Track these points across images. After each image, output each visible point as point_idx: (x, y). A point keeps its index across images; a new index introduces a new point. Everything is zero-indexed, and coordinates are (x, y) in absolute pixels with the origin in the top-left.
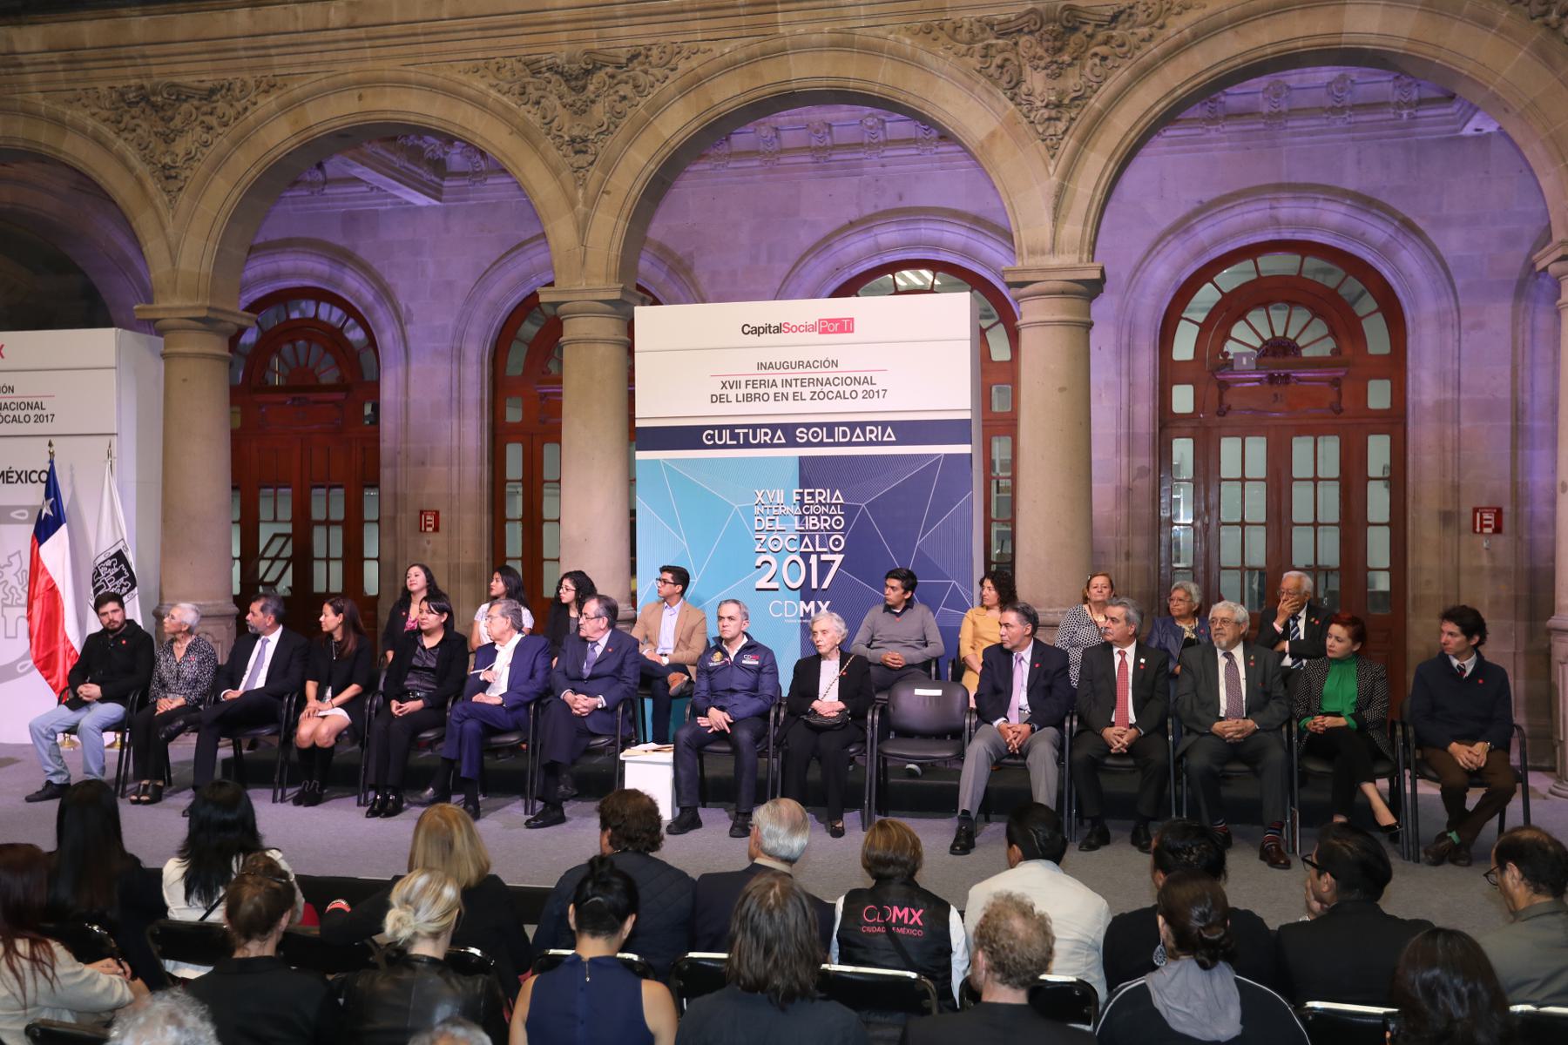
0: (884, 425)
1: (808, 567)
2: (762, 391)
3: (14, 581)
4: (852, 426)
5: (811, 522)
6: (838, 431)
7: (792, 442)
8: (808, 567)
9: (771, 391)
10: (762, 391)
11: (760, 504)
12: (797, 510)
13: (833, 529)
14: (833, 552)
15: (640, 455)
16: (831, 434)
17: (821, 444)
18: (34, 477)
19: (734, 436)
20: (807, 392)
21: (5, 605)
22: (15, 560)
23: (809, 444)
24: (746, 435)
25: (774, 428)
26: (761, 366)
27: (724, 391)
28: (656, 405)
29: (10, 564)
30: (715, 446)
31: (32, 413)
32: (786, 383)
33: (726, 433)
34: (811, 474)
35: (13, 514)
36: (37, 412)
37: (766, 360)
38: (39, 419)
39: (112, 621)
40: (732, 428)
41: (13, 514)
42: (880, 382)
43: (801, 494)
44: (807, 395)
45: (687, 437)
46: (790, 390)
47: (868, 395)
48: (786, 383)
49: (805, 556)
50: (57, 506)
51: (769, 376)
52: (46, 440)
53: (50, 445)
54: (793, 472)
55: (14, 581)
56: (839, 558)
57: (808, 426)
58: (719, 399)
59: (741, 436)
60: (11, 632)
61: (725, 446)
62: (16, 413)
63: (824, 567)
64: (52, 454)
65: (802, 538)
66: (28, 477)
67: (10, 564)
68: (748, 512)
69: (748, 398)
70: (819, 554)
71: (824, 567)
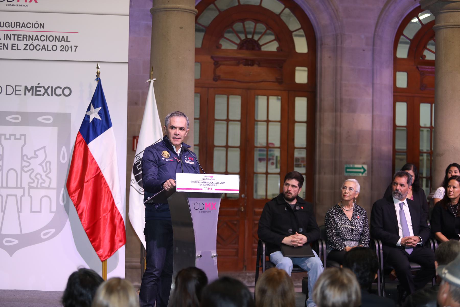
3: (39, 169)
18: (59, 91)
21: (30, 188)
22: (41, 154)
29: (37, 157)
31: (59, 44)
35: (40, 119)
36: (63, 43)
38: (64, 49)
39: (288, 192)
41: (40, 119)
50: (105, 113)
52: (95, 65)
53: (98, 67)
55: (39, 169)
60: (36, 208)
62: (46, 43)
64: (98, 73)
66: (54, 91)
67: (37, 157)
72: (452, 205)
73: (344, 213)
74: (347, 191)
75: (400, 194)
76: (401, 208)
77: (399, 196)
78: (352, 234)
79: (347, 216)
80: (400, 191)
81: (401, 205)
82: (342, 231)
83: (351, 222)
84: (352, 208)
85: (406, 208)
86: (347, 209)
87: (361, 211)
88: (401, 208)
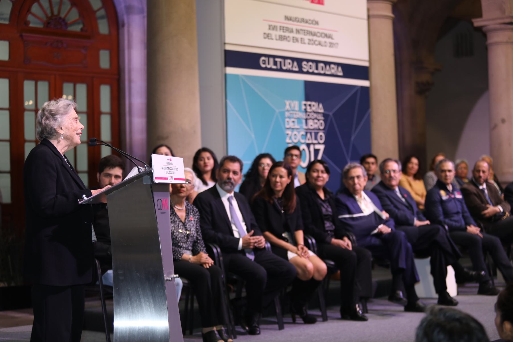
0: (338, 64)
1: (310, 152)
2: (287, 34)
4: (326, 63)
5: (310, 122)
6: (321, 65)
7: (301, 71)
8: (310, 152)
9: (291, 35)
10: (287, 34)
11: (288, 111)
12: (303, 115)
13: (319, 129)
14: (319, 143)
15: (231, 71)
16: (317, 68)
17: (313, 73)
19: (275, 63)
20: (307, 38)
23: (308, 73)
24: (281, 62)
25: (293, 59)
26: (287, 18)
27: (270, 32)
28: (240, 35)
30: (266, 69)
32: (298, 31)
33: (271, 60)
34: (313, 92)
37: (289, 15)
40: (274, 57)
42: (334, 37)
43: (305, 105)
44: (307, 41)
45: (250, 60)
46: (299, 36)
47: (332, 45)
48: (298, 31)
49: (308, 145)
51: (294, 26)
54: (301, 91)
56: (322, 147)
57: (308, 61)
58: (267, 36)
59: (278, 63)
61: (271, 69)
63: (317, 151)
65: (307, 133)
68: (282, 114)
69: (282, 38)
70: (314, 144)
71: (317, 151)
72: (276, 198)
73: (176, 214)
74: (278, 179)
75: (232, 184)
76: (231, 204)
77: (231, 187)
78: (187, 241)
79: (180, 217)
80: (232, 180)
81: (231, 199)
82: (176, 237)
83: (184, 225)
84: (184, 208)
85: (235, 203)
86: (180, 208)
87: (193, 210)
88: (231, 204)
